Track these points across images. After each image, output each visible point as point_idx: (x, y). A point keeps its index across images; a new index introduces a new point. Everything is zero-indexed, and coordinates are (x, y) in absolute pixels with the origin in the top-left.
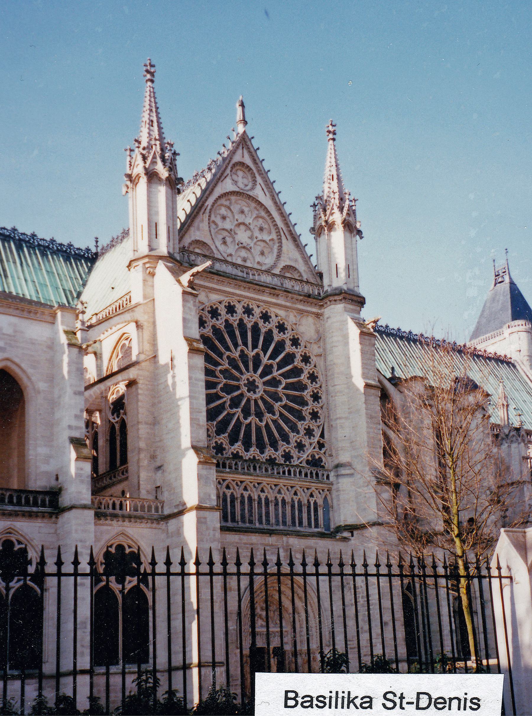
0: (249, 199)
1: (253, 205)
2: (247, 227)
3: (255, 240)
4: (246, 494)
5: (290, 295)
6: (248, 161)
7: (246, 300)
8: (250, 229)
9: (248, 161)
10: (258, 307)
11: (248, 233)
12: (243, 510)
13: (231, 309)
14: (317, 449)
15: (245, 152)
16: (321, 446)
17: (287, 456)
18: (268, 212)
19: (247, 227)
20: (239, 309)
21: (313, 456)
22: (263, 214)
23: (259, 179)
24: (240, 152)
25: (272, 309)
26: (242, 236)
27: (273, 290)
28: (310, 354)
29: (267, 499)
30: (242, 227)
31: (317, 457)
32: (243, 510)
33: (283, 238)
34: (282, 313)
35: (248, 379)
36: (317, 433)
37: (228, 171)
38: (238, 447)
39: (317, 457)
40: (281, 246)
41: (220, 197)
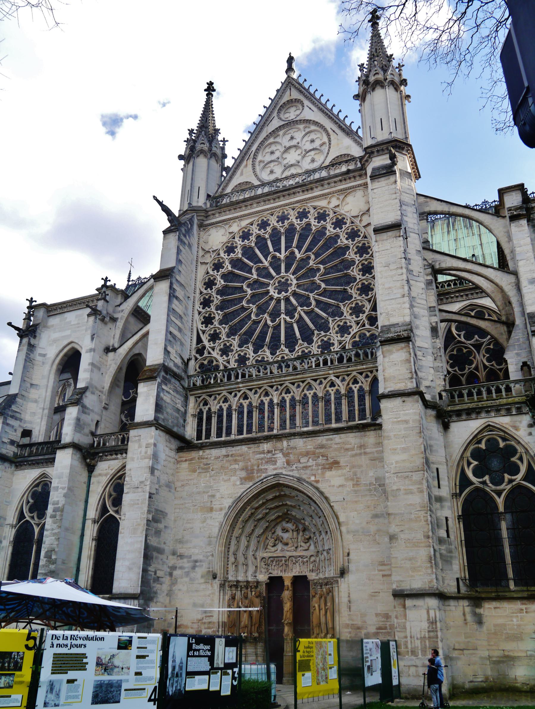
0: (297, 124)
1: (301, 126)
2: (296, 147)
3: (304, 153)
4: (266, 400)
5: (326, 182)
6: (295, 95)
7: (278, 209)
8: (300, 148)
9: (295, 95)
10: (293, 209)
11: (299, 151)
12: (262, 419)
13: (264, 225)
14: (367, 326)
15: (292, 89)
16: (373, 320)
17: (326, 346)
18: (316, 123)
19: (296, 147)
20: (273, 221)
21: (363, 336)
22: (313, 127)
23: (306, 102)
24: (288, 92)
25: (309, 205)
26: (292, 157)
27: (305, 187)
28: (359, 228)
29: (293, 399)
30: (292, 151)
31: (368, 334)
32: (262, 419)
33: (333, 136)
34: (322, 203)
35: (279, 282)
36: (368, 307)
37: (275, 114)
38: (266, 354)
39: (368, 334)
40: (330, 144)
41: (266, 139)
